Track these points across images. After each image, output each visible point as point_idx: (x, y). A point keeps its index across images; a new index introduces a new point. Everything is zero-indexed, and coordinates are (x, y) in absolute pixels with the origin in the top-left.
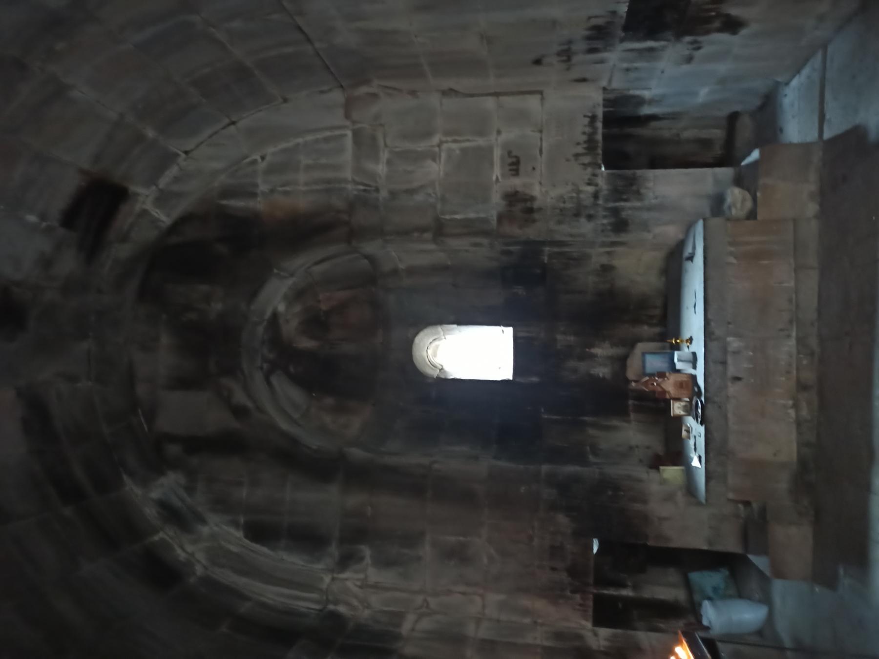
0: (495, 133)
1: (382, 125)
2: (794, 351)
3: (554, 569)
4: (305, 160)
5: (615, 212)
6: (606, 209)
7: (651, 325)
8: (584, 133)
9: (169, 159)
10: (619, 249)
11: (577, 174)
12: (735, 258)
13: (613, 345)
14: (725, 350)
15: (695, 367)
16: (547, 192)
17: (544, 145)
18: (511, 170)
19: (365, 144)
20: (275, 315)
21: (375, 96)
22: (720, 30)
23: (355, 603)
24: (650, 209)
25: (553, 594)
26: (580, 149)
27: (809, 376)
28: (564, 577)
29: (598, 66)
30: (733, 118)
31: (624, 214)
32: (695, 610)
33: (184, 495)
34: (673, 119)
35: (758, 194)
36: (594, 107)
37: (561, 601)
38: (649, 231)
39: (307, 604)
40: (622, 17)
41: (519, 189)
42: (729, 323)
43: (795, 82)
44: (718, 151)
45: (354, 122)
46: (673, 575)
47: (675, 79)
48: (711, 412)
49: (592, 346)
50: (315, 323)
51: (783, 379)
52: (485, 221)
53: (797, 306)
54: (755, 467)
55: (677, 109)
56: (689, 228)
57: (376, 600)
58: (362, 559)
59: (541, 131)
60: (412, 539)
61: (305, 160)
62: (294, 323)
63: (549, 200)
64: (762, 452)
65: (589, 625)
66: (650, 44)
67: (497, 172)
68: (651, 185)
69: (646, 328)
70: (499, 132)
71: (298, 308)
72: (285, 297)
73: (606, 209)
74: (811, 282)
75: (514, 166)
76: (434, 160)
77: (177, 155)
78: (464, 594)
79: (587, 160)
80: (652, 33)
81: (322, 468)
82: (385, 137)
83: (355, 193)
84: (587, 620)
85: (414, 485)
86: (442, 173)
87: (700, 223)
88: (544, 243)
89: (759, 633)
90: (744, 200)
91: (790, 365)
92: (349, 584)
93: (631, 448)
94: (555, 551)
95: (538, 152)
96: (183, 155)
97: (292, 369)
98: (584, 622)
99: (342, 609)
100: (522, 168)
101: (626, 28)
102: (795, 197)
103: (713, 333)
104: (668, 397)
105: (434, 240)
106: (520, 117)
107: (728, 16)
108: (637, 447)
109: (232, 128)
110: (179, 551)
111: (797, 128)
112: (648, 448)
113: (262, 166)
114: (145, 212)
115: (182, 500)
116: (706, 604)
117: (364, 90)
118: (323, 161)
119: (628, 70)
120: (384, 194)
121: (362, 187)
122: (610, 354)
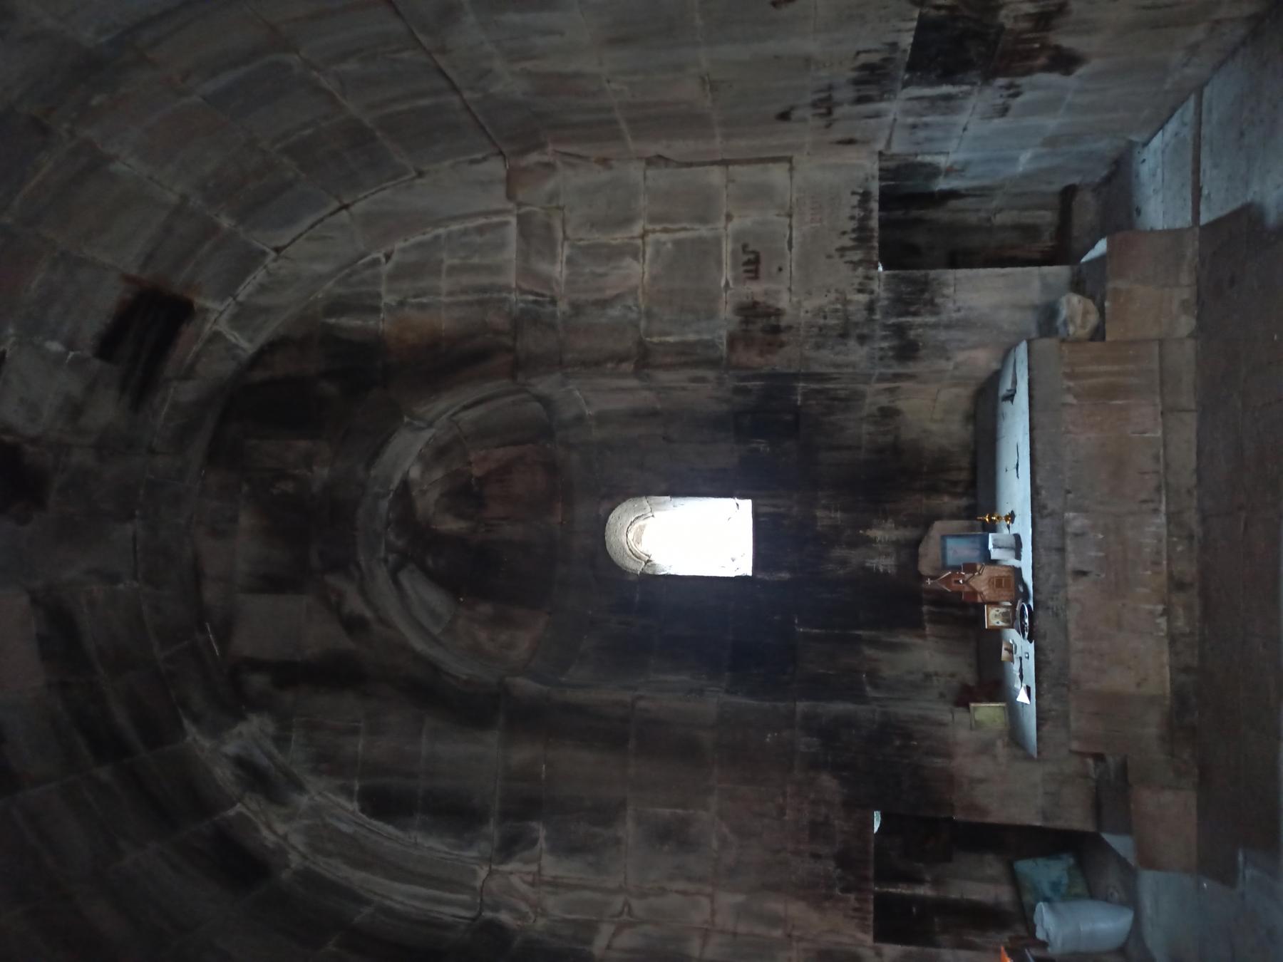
0: (723, 218)
1: (559, 208)
2: (1164, 531)
3: (816, 856)
4: (448, 261)
5: (900, 330)
6: (886, 327)
7: (954, 495)
8: (852, 218)
9: (252, 258)
10: (905, 385)
11: (843, 276)
12: (1076, 396)
13: (899, 524)
14: (1062, 532)
15: (1018, 557)
16: (799, 302)
17: (794, 234)
18: (747, 271)
19: (536, 235)
20: (406, 484)
21: (549, 166)
22: (1047, 69)
23: (524, 907)
24: (949, 326)
25: (815, 893)
26: (847, 241)
27: (1187, 569)
28: (831, 865)
29: (872, 121)
30: (1069, 193)
31: (912, 334)
32: (1026, 918)
33: (275, 751)
34: (980, 196)
35: (1107, 304)
36: (867, 179)
37: (827, 904)
38: (948, 359)
39: (453, 909)
40: (905, 51)
41: (760, 299)
42: (1069, 492)
43: (1156, 142)
44: (1046, 242)
45: (520, 205)
46: (993, 866)
47: (982, 141)
48: (1044, 622)
49: (868, 526)
50: (465, 494)
51: (1149, 573)
52: (710, 345)
53: (1167, 466)
54: (1110, 704)
55: (986, 182)
56: (1007, 353)
57: (554, 904)
58: (534, 842)
59: (790, 216)
60: (607, 813)
61: (448, 261)
62: (434, 495)
63: (802, 314)
64: (1120, 680)
65: (868, 939)
66: (946, 89)
67: (727, 274)
68: (949, 291)
69: (946, 499)
70: (729, 217)
71: (438, 474)
72: (421, 457)
73: (886, 327)
74: (1187, 431)
75: (752, 266)
76: (635, 257)
77: (264, 254)
78: (684, 893)
79: (857, 256)
80: (948, 76)
81: (474, 708)
82: (564, 223)
83: (521, 305)
84: (866, 932)
85: (612, 732)
86: (646, 276)
87: (1022, 349)
88: (796, 377)
89: (1122, 951)
90: (1086, 313)
91: (1158, 553)
92: (515, 880)
93: (928, 676)
94: (818, 830)
95: (786, 246)
96: (273, 254)
97: (430, 562)
98: (861, 936)
99: (505, 917)
100: (763, 268)
101: (911, 67)
102: (1161, 309)
103: (1045, 507)
104: (979, 600)
105: (636, 373)
106: (759, 195)
107: (1058, 48)
108: (936, 674)
109: (344, 212)
110: (265, 832)
111: (1160, 208)
112: (953, 675)
113: (386, 268)
114: (217, 336)
115: (270, 757)
116: (1042, 907)
117: (534, 158)
118: (476, 260)
119: (914, 126)
120: (563, 306)
121: (531, 298)
122: (894, 538)
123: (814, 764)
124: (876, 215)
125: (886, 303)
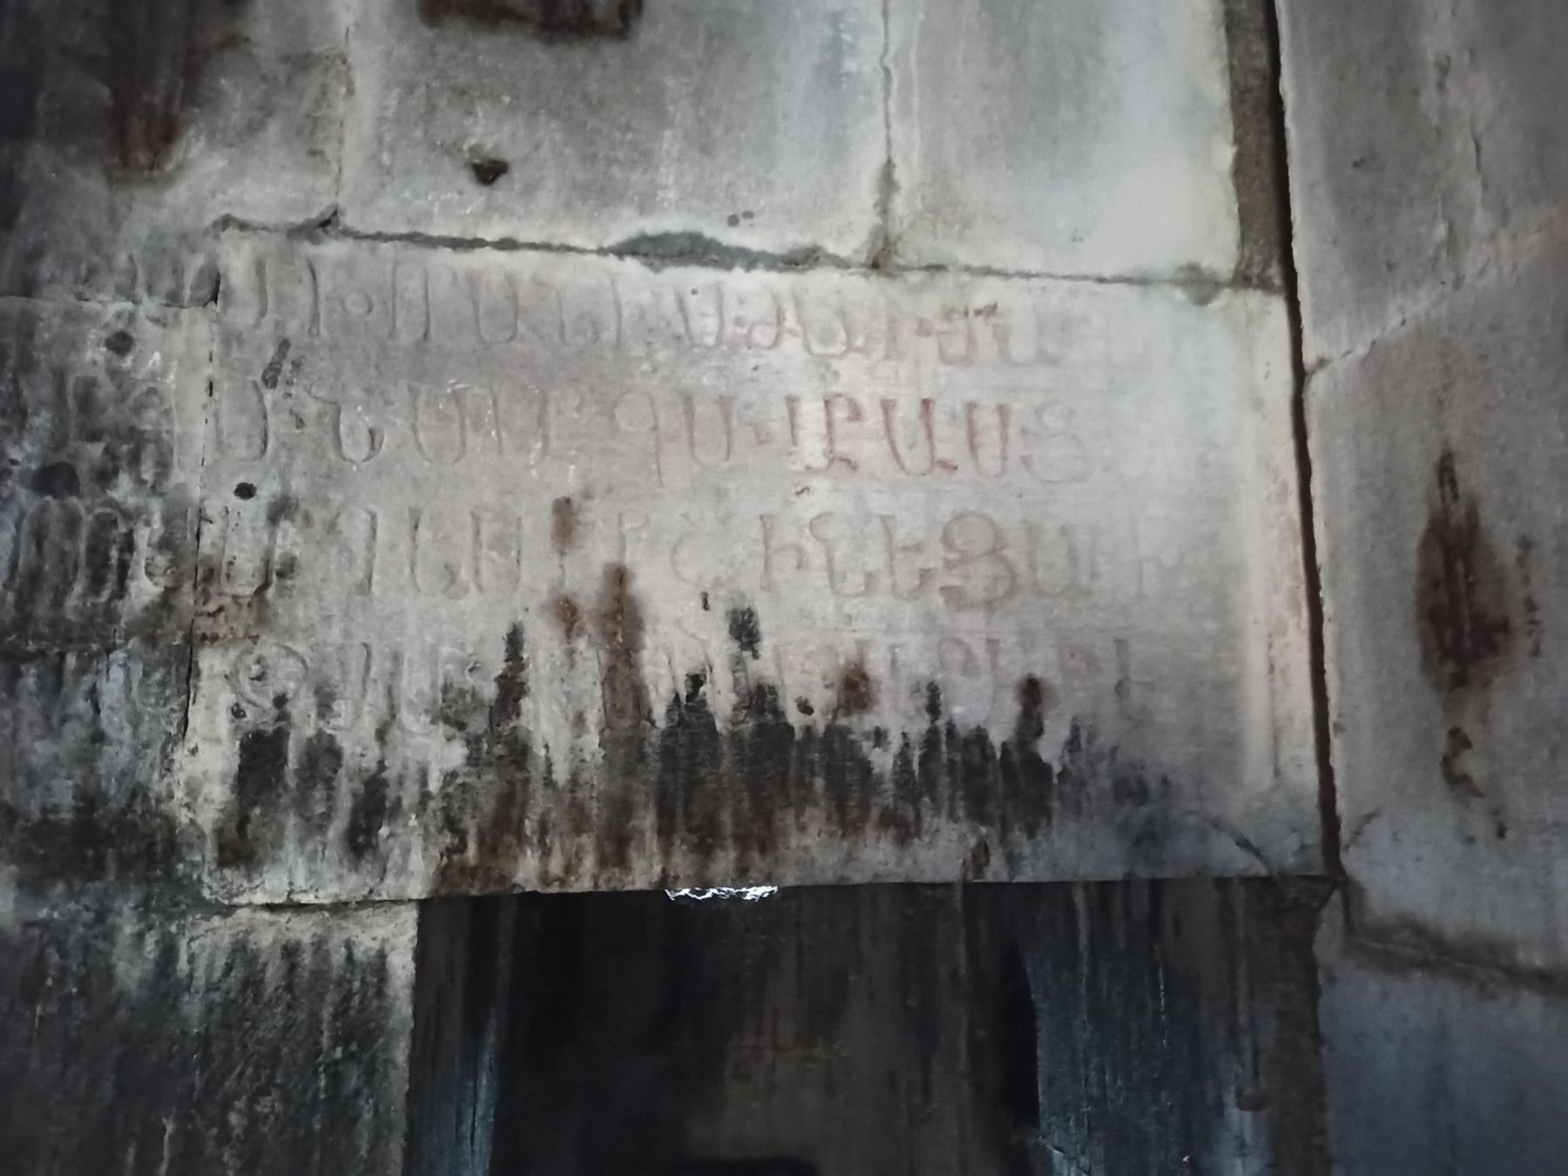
8: (855, 689)
16: (214, 289)
17: (738, 279)
26: (680, 644)
59: (880, 262)
63: (109, 308)
79: (561, 724)
124: (878, 857)
125: (131, 970)
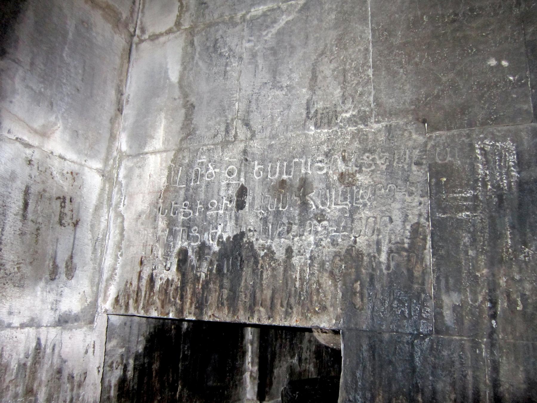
28: (227, 231)
37: (162, 224)
94: (293, 192)
123: (441, 180)
